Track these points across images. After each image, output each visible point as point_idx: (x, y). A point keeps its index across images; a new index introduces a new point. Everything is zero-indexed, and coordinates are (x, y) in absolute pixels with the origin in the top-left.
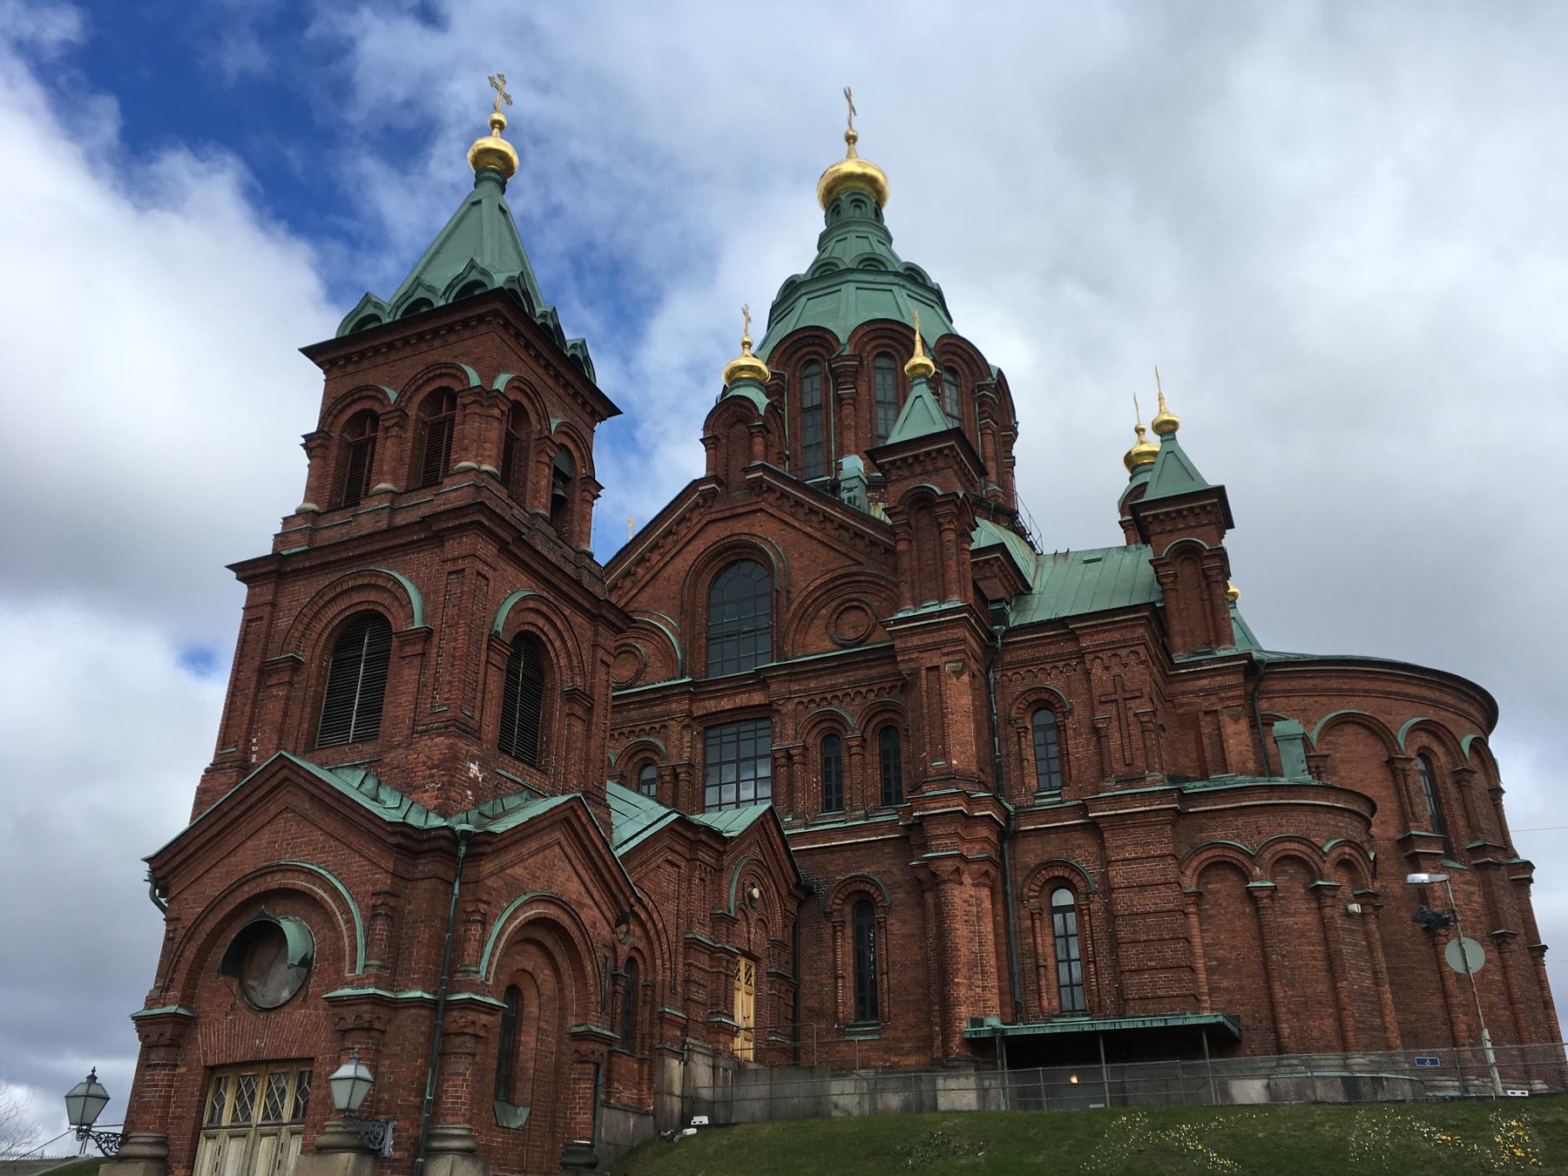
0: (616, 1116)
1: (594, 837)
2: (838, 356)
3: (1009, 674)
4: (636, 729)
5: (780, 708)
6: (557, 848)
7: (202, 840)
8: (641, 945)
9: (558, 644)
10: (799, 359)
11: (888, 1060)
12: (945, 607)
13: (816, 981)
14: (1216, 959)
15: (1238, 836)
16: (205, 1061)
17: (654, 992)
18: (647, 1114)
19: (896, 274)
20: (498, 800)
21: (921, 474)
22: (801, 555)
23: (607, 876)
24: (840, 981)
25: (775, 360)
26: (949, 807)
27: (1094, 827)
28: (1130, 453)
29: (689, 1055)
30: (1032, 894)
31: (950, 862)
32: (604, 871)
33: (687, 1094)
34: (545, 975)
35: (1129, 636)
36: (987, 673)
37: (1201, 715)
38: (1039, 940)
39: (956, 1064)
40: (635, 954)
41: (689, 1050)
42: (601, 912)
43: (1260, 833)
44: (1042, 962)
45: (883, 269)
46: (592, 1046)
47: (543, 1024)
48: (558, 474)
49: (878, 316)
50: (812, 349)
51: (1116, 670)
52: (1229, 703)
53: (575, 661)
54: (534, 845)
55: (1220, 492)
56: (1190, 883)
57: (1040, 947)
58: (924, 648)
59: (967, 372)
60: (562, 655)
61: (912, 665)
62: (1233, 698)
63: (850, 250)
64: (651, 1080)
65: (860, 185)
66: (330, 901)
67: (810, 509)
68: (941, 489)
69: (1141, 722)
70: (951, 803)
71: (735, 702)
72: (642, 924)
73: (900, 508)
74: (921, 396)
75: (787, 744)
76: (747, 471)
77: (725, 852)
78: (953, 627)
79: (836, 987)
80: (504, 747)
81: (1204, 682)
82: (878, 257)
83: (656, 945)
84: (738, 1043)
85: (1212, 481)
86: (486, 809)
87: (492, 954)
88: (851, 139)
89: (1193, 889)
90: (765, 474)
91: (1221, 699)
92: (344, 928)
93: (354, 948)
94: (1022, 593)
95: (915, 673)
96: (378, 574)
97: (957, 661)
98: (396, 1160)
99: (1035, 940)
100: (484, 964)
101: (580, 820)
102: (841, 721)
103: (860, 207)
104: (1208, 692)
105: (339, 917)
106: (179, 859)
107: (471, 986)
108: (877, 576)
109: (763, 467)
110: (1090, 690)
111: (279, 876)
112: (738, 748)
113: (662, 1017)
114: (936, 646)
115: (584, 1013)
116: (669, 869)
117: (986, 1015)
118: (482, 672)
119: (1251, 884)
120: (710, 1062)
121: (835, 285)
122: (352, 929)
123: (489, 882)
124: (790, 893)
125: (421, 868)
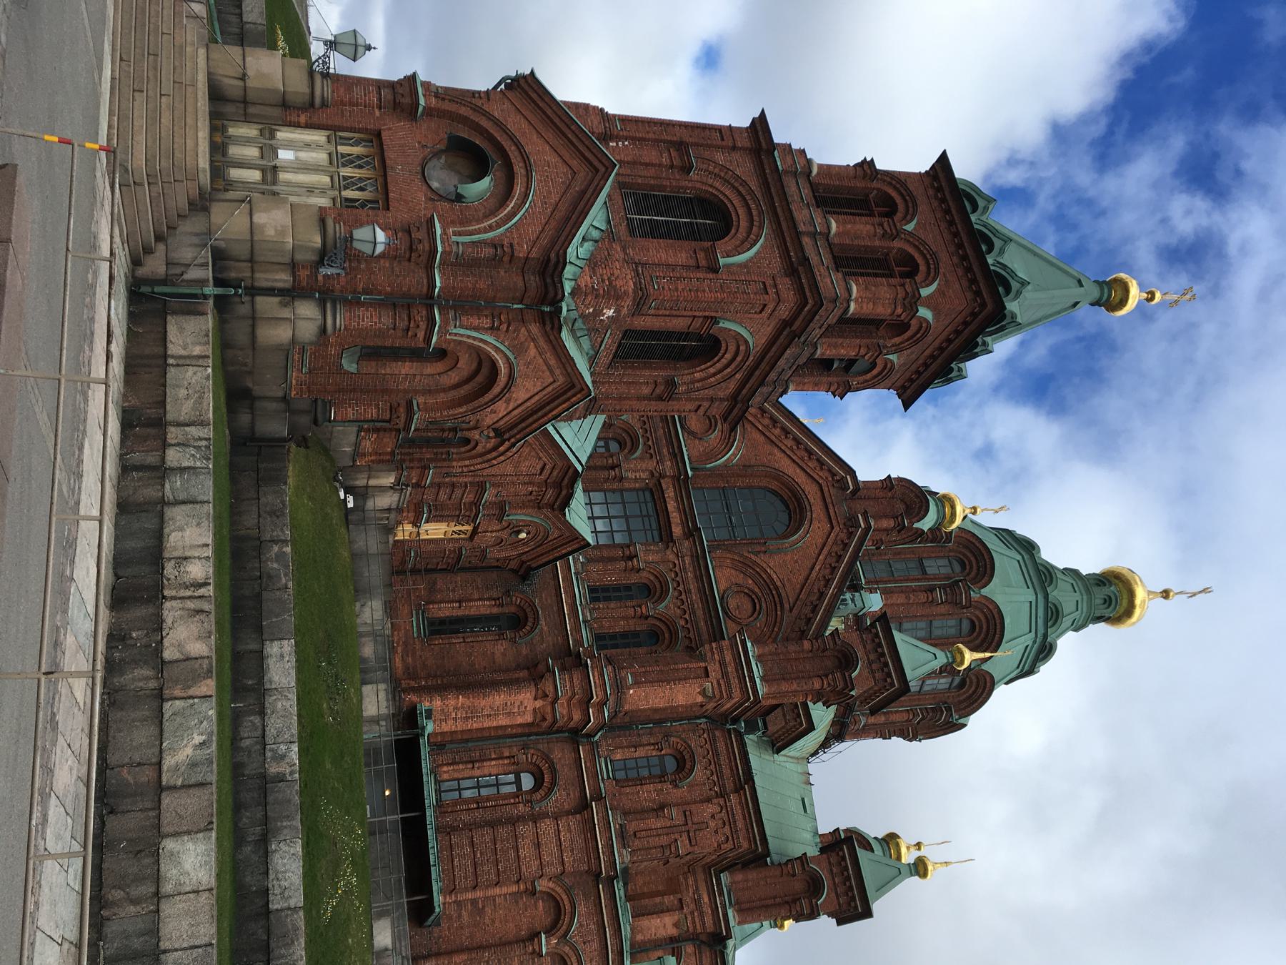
0: (352, 438)
1: (560, 408)
2: (969, 588)
3: (705, 735)
4: (648, 435)
5: (670, 548)
6: (552, 380)
7: (549, 112)
8: (480, 449)
9: (712, 370)
10: (964, 555)
11: (398, 644)
12: (758, 681)
13: (456, 586)
14: (483, 907)
15: (581, 926)
16: (384, 130)
17: (444, 460)
18: (354, 461)
19: (1045, 636)
20: (586, 333)
21: (868, 659)
22: (796, 562)
23: (531, 420)
24: (457, 604)
25: (963, 535)
26: (595, 688)
27: (584, 806)
28: (899, 837)
29: (397, 489)
30: (529, 756)
31: (552, 689)
33: (369, 490)
34: (454, 377)
35: (741, 835)
36: (705, 717)
37: (679, 896)
38: (493, 763)
39: (397, 698)
40: (473, 444)
41: (402, 489)
42: (503, 417)
43: (584, 943)
44: (477, 765)
45: (1050, 624)
46: (403, 416)
47: (418, 378)
48: (851, 362)
49: (1007, 621)
51: (712, 824)
52: (689, 919)
53: (697, 385)
54: (552, 362)
55: (867, 913)
56: (543, 885)
57: (488, 763)
58: (722, 664)
60: (703, 375)
61: (709, 655)
62: (694, 922)
63: (1064, 595)
64: (379, 462)
65: (1125, 603)
66: (506, 212)
67: (835, 568)
70: (598, 689)
71: (673, 512)
72: (495, 448)
73: (839, 642)
74: (936, 658)
75: (641, 555)
76: (865, 515)
77: (553, 510)
79: (452, 602)
80: (628, 334)
81: (706, 899)
82: (1060, 620)
83: (480, 460)
84: (408, 527)
85: (876, 907)
86: (579, 324)
87: (469, 337)
88: (1166, 594)
89: (538, 888)
90: (862, 529)
91: (692, 913)
92: (485, 224)
93: (471, 233)
94: (773, 745)
95: (703, 658)
96: (761, 227)
97: (713, 692)
98: (316, 276)
99: (494, 759)
100: (462, 331)
101: (574, 395)
102: (662, 598)
103: (1104, 603)
104: (698, 902)
105: (493, 220)
106: (534, 96)
107: (445, 323)
108: (781, 625)
109: (868, 528)
110: (695, 802)
111: (523, 171)
112: (637, 516)
113: (425, 468)
114: (725, 674)
115: (427, 409)
116: (539, 467)
117: (434, 722)
118: (685, 313)
119: (543, 936)
120: (394, 506)
121: (1032, 583)
122: (485, 231)
123: (523, 329)
124: (523, 562)
125: (532, 278)
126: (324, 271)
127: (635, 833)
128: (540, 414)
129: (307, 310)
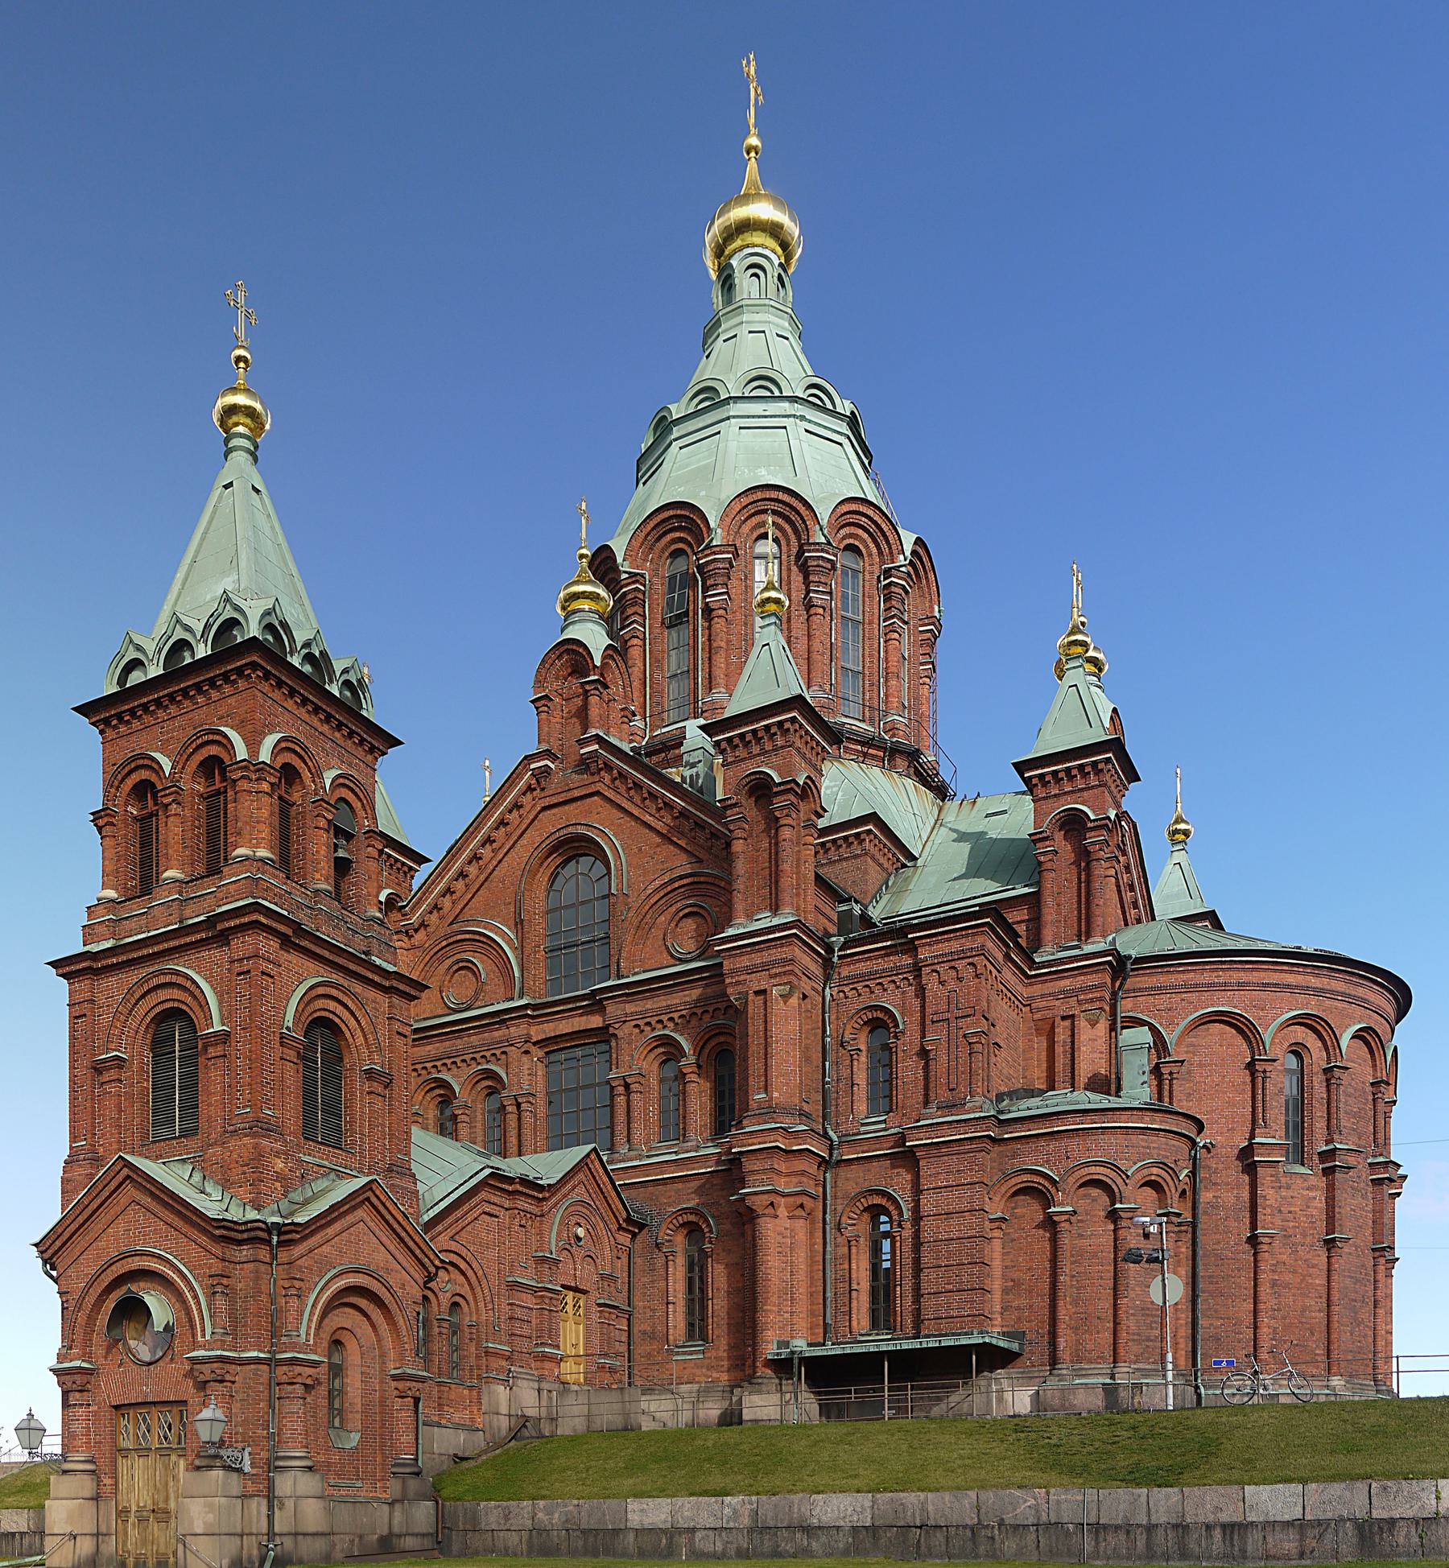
1: (394, 1212)
2: (708, 547)
3: (846, 989)
7: (73, 1227)
12: (776, 921)
13: (649, 1307)
16: (110, 1402)
20: (307, 1185)
23: (411, 1244)
29: (513, 1382)
31: (766, 1196)
32: (407, 1239)
41: (513, 1377)
50: (677, 535)
51: (952, 985)
58: (752, 970)
59: (874, 550)
60: (359, 1033)
62: (1092, 1000)
66: (179, 1281)
68: (780, 775)
69: (970, 1044)
78: (782, 946)
80: (308, 1133)
84: (567, 1367)
86: (296, 1196)
87: (310, 1320)
92: (192, 1303)
93: (202, 1319)
97: (785, 984)
98: (253, 1475)
104: (1068, 994)
105: (188, 1294)
106: (58, 1243)
107: (293, 1347)
108: (716, 877)
110: (923, 1007)
115: (401, 1357)
119: (1053, 1209)
122: (198, 1303)
125: (245, 1253)
126: (247, 1469)
127: (950, 1090)
128: (403, 1234)
129: (285, 1484)
